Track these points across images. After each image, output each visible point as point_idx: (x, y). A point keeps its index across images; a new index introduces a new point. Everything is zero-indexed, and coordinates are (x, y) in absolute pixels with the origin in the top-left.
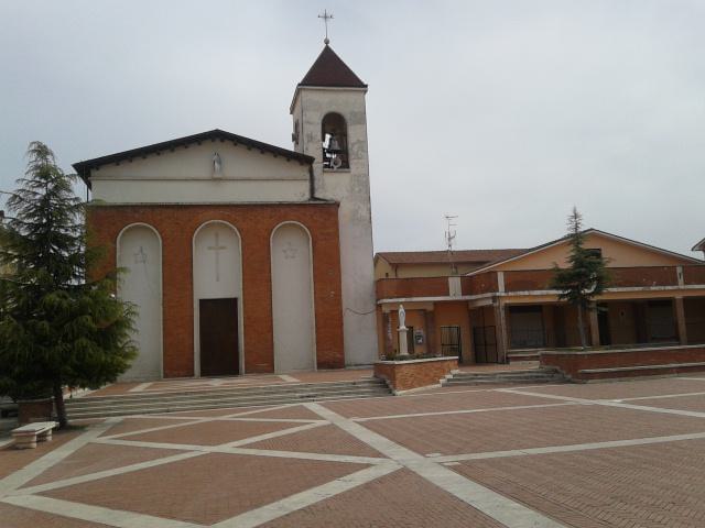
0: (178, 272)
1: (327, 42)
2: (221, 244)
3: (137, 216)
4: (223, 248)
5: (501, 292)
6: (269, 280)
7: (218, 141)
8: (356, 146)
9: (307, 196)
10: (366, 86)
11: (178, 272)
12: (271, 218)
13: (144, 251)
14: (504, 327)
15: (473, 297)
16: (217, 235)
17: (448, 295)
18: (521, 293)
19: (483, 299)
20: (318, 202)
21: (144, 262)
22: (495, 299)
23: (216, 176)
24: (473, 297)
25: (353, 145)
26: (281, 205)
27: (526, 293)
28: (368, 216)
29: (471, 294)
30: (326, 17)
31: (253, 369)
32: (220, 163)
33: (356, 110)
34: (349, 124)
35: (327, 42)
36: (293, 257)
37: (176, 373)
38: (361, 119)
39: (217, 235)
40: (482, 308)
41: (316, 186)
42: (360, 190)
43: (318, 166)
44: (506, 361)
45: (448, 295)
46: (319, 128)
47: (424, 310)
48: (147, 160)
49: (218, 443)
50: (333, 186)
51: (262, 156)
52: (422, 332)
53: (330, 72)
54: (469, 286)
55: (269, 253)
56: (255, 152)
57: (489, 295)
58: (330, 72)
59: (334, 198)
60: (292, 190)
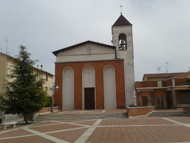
0: (78, 80)
1: (121, 13)
2: (90, 72)
3: (68, 65)
4: (91, 73)
5: (174, 86)
6: (103, 82)
7: (89, 44)
8: (129, 43)
9: (114, 58)
10: (132, 25)
11: (78, 80)
12: (104, 64)
13: (70, 75)
14: (175, 97)
15: (166, 87)
16: (89, 70)
17: (158, 87)
18: (181, 86)
19: (168, 88)
20: (117, 59)
21: (70, 78)
22: (172, 88)
23: (89, 53)
24: (166, 87)
25: (128, 42)
26: (106, 61)
27: (182, 86)
28: (132, 63)
29: (165, 87)
30: (121, 6)
31: (98, 108)
32: (90, 50)
33: (129, 32)
34: (126, 36)
35: (121, 13)
36: (110, 76)
37: (77, 108)
38: (131, 34)
39: (89, 70)
40: (169, 90)
41: (117, 55)
42: (130, 55)
43: (117, 49)
44: (176, 108)
45: (158, 87)
46: (118, 38)
47: (150, 91)
48: (68, 51)
49: (186, 123)
50: (122, 55)
51: (101, 47)
52: (150, 98)
53: (122, 22)
54: (164, 84)
55: (103, 74)
56: (100, 46)
57: (170, 87)
58: (122, 22)
59: (122, 58)
60: (110, 56)
